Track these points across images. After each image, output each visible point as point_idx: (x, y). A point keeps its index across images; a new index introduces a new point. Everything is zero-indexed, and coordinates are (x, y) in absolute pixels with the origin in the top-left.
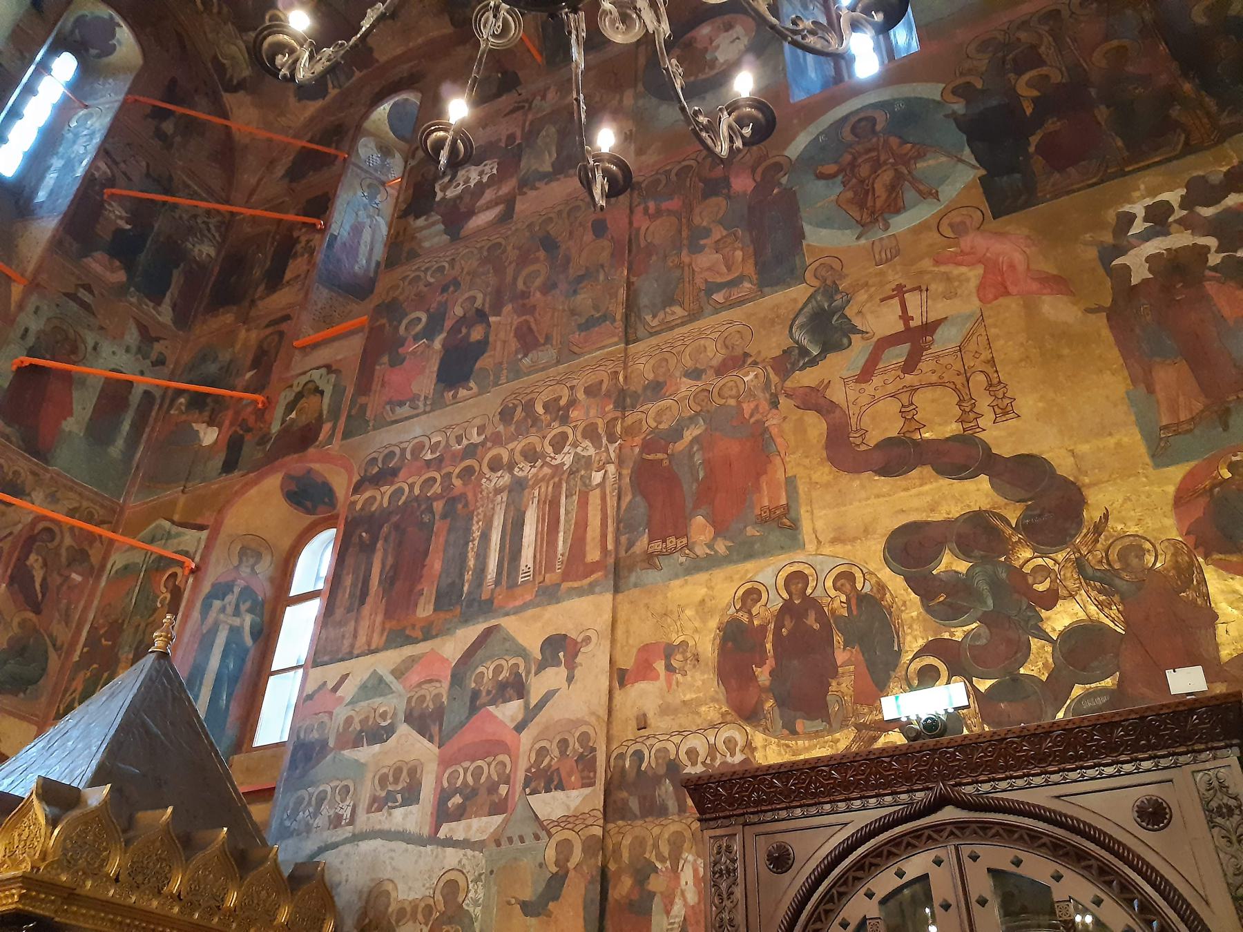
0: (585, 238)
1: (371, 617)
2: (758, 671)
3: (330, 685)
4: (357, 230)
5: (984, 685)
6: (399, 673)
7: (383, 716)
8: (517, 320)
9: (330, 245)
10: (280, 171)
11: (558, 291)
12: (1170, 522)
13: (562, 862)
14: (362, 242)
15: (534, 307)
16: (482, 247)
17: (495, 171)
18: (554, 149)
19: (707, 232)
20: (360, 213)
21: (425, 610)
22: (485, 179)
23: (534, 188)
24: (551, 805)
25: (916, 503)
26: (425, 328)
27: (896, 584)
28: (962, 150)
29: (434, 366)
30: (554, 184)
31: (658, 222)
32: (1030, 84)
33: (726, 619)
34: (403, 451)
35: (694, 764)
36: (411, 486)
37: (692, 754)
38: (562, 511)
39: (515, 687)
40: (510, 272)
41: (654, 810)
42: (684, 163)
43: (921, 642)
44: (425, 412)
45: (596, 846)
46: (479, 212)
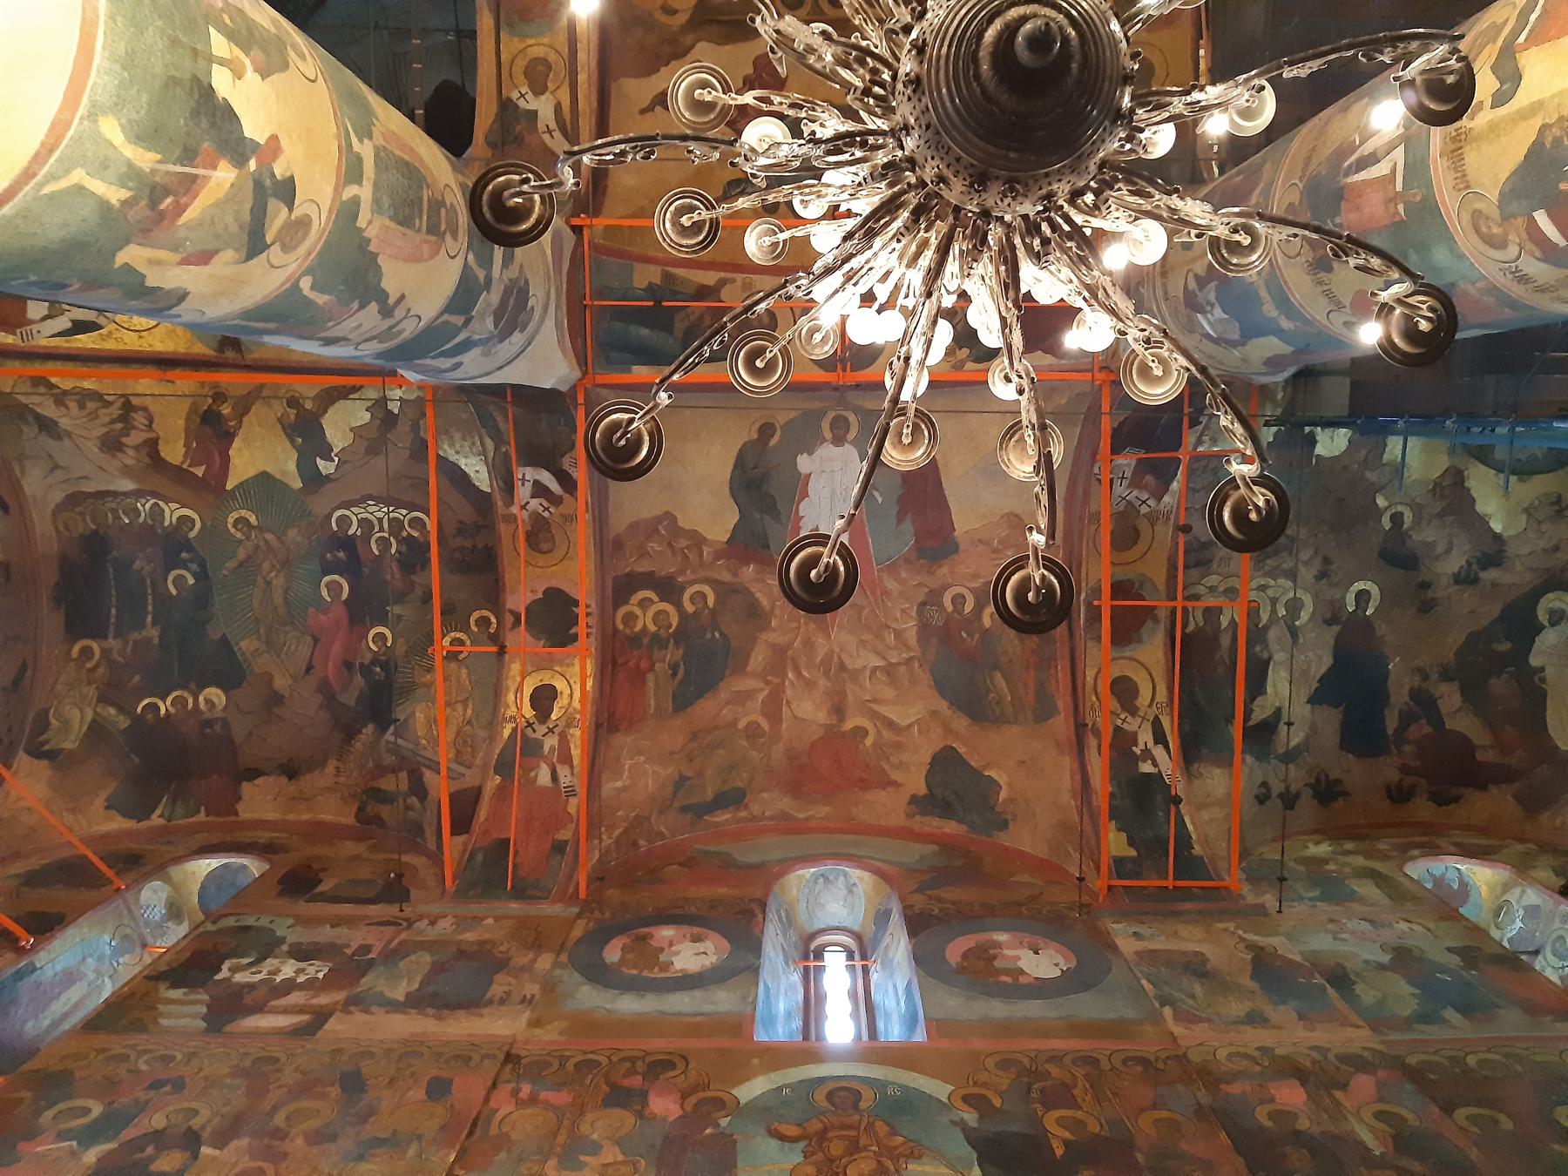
0: (411, 1093)
4: (70, 978)
8: (246, 1163)
9: (20, 975)
10: (19, 867)
11: (332, 1147)
14: (63, 997)
15: (285, 1155)
16: (247, 1054)
17: (321, 975)
18: (418, 979)
19: (595, 1149)
20: (90, 960)
22: (301, 979)
23: (366, 1011)
26: (88, 1127)
28: (971, 1168)
30: (398, 1017)
31: (529, 1111)
32: (1060, 1122)
40: (274, 1096)
42: (590, 1056)
46: (270, 1012)
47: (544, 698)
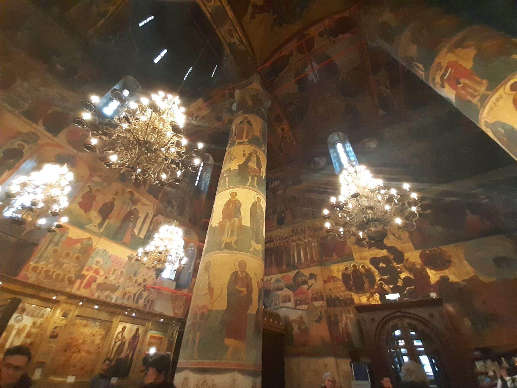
1: (274, 269)
2: (350, 282)
3: (269, 279)
5: (391, 286)
6: (282, 278)
7: (281, 286)
12: (420, 260)
13: (321, 313)
17: (280, 183)
21: (284, 267)
24: (317, 304)
25: (374, 253)
27: (373, 268)
29: (276, 221)
33: (343, 272)
34: (274, 237)
35: (342, 297)
36: (277, 244)
37: (341, 296)
38: (308, 251)
39: (305, 282)
41: (335, 305)
43: (379, 279)
44: (275, 230)
45: (326, 311)
47: (283, 130)
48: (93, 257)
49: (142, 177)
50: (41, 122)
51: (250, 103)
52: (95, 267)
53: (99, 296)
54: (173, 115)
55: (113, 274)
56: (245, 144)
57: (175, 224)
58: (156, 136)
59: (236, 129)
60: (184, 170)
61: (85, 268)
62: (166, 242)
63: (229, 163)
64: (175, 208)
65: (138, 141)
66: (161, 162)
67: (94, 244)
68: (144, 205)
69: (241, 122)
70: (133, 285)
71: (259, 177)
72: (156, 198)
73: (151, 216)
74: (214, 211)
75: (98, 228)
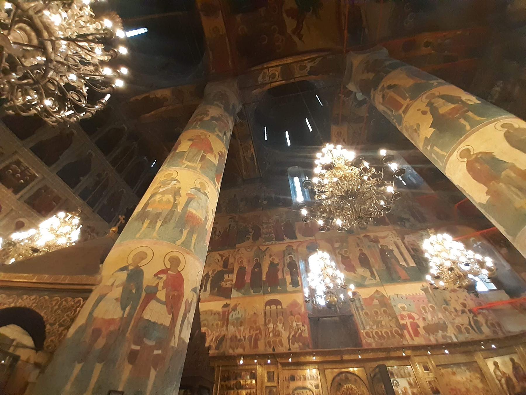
47: (427, 44)
48: (395, 306)
49: (371, 218)
50: (285, 238)
51: (371, 76)
52: (405, 313)
53: (437, 340)
54: (340, 158)
55: (426, 312)
56: (411, 105)
57: (431, 233)
58: (346, 182)
59: (386, 107)
60: (393, 183)
61: (399, 318)
62: (444, 254)
63: (419, 136)
64: (412, 219)
65: (342, 197)
66: (370, 195)
67: (385, 294)
68: (384, 238)
69: (383, 97)
70: (457, 315)
71: (474, 109)
72: (387, 224)
73: (399, 242)
74: (462, 189)
75: (374, 280)
